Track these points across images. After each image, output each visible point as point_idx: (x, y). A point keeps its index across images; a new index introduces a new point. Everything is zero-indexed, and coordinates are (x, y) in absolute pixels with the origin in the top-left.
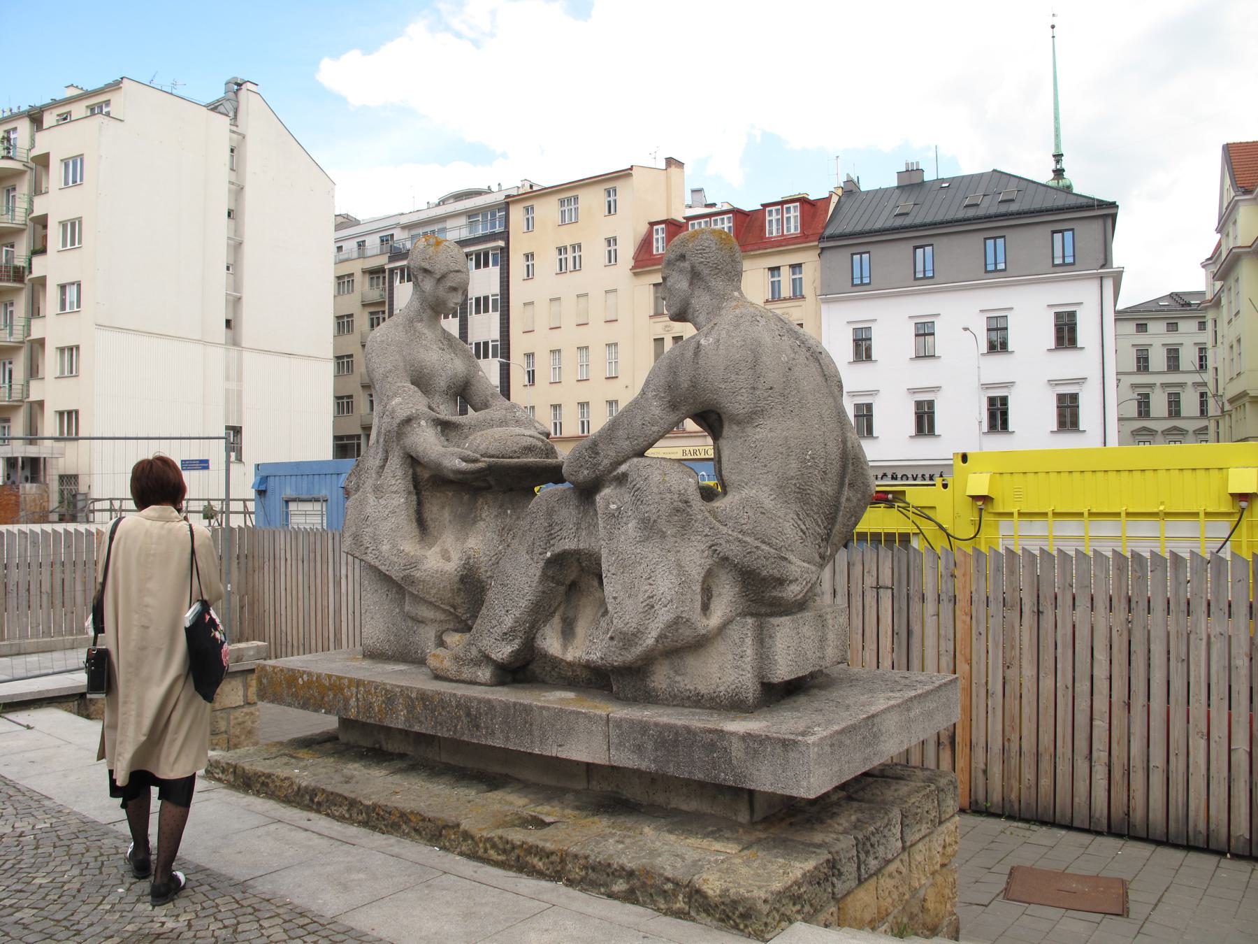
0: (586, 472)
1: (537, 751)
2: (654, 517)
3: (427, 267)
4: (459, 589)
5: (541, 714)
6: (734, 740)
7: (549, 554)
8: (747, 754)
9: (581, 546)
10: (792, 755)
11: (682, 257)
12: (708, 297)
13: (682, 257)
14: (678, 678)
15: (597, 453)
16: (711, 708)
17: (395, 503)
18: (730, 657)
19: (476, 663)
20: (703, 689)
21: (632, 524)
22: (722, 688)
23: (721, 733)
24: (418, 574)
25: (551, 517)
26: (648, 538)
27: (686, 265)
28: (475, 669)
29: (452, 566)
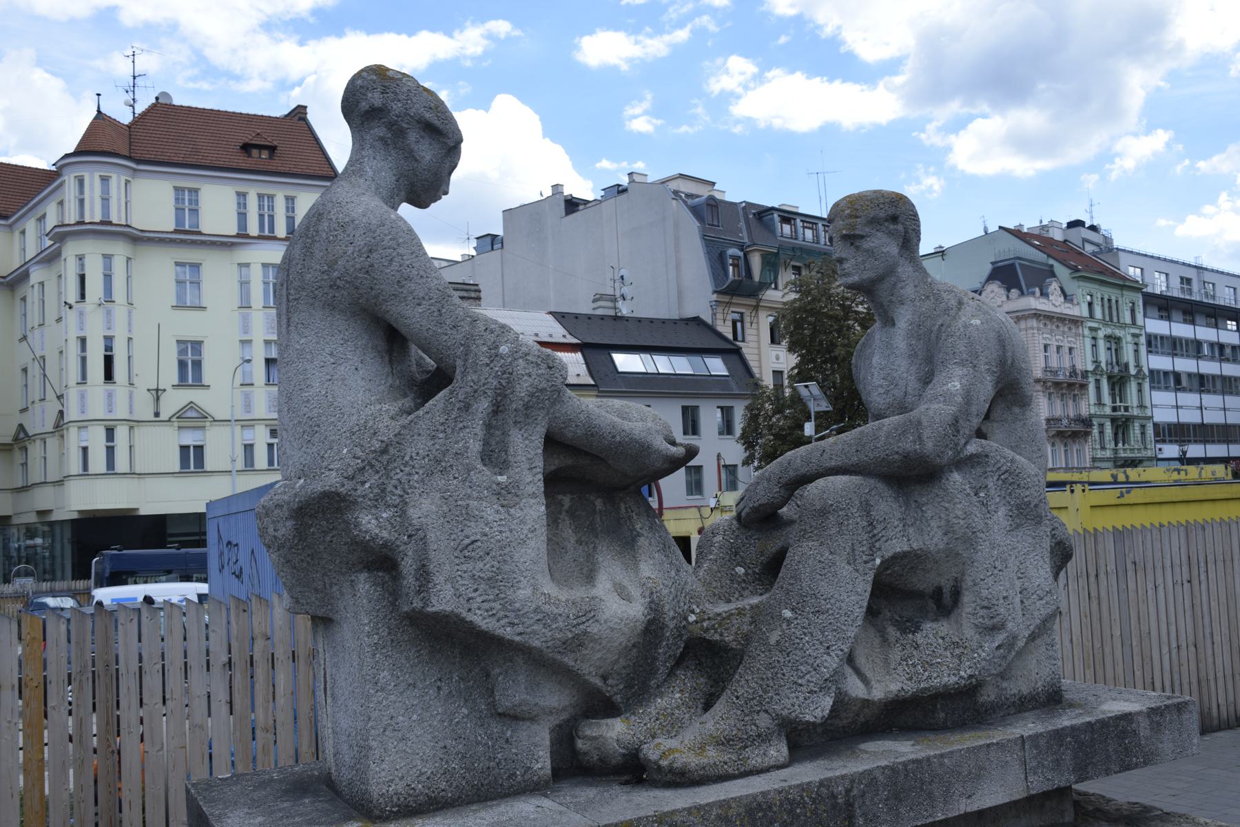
0: (950, 453)
1: (940, 816)
2: (1036, 501)
3: (436, 122)
4: (634, 646)
5: (942, 764)
6: (1140, 719)
7: (878, 561)
8: (1152, 729)
9: (915, 546)
10: (1185, 716)
11: (894, 219)
12: (910, 269)
13: (894, 219)
14: (1005, 684)
15: (958, 431)
16: (1033, 708)
17: (535, 515)
18: (1043, 649)
19: (763, 738)
20: (1025, 690)
21: (1002, 512)
22: (1040, 684)
23: (1127, 717)
24: (594, 629)
25: (868, 514)
26: (1018, 526)
27: (900, 227)
28: (764, 746)
29: (636, 610)
